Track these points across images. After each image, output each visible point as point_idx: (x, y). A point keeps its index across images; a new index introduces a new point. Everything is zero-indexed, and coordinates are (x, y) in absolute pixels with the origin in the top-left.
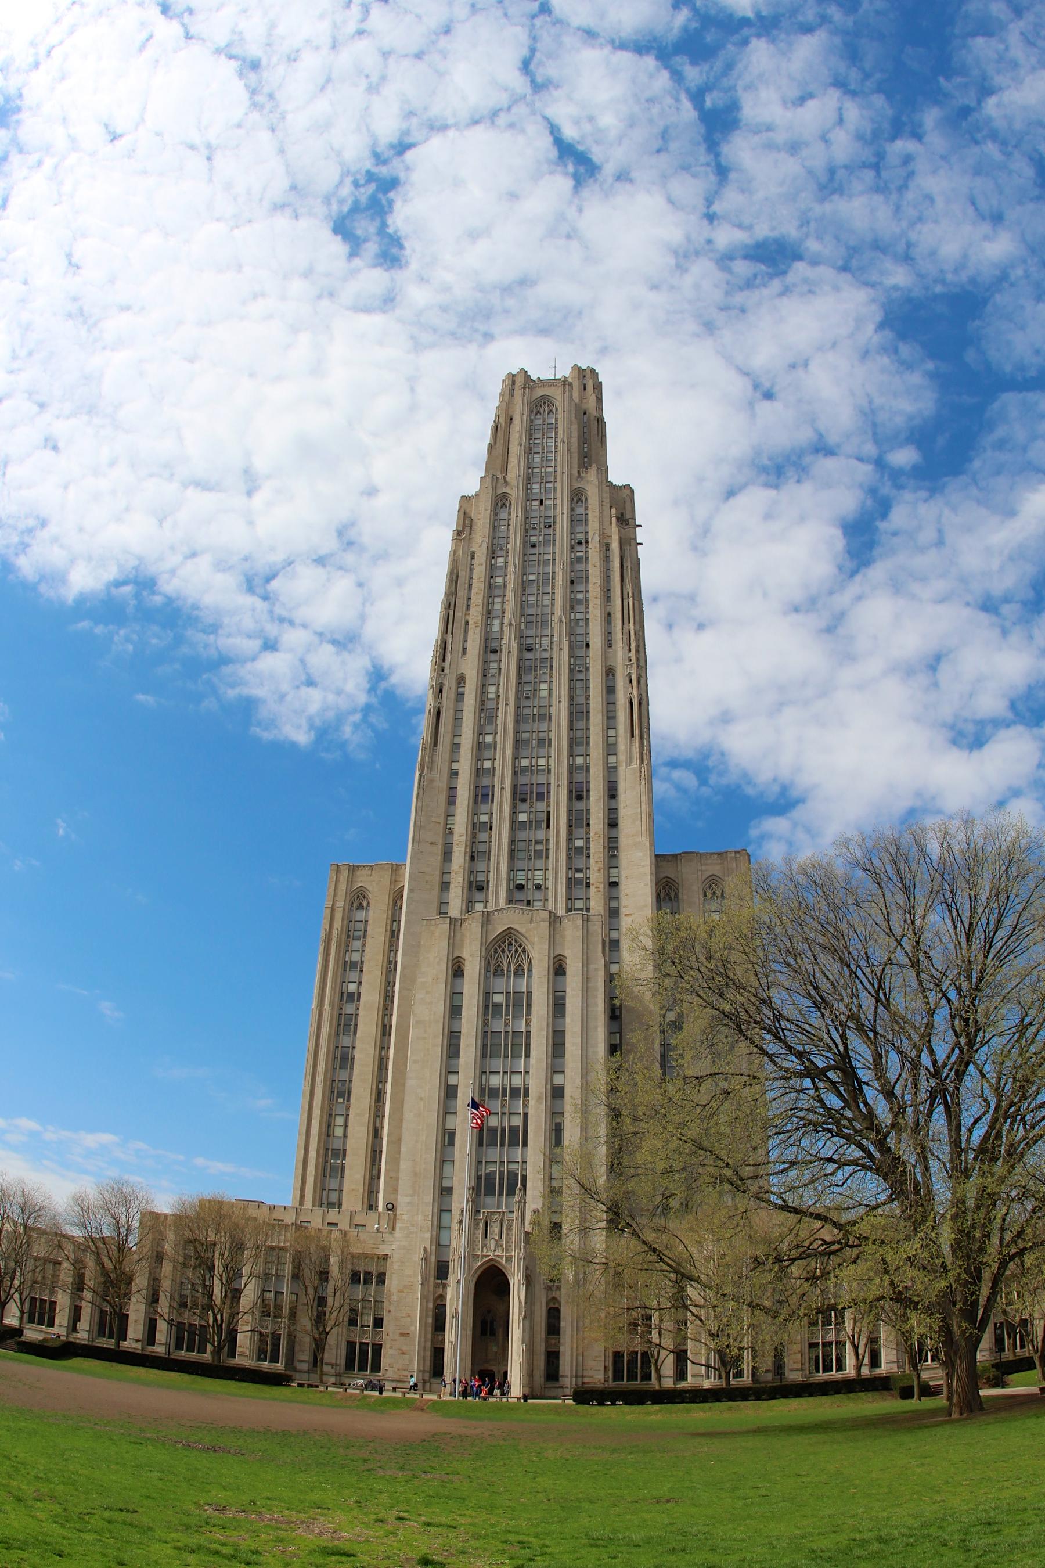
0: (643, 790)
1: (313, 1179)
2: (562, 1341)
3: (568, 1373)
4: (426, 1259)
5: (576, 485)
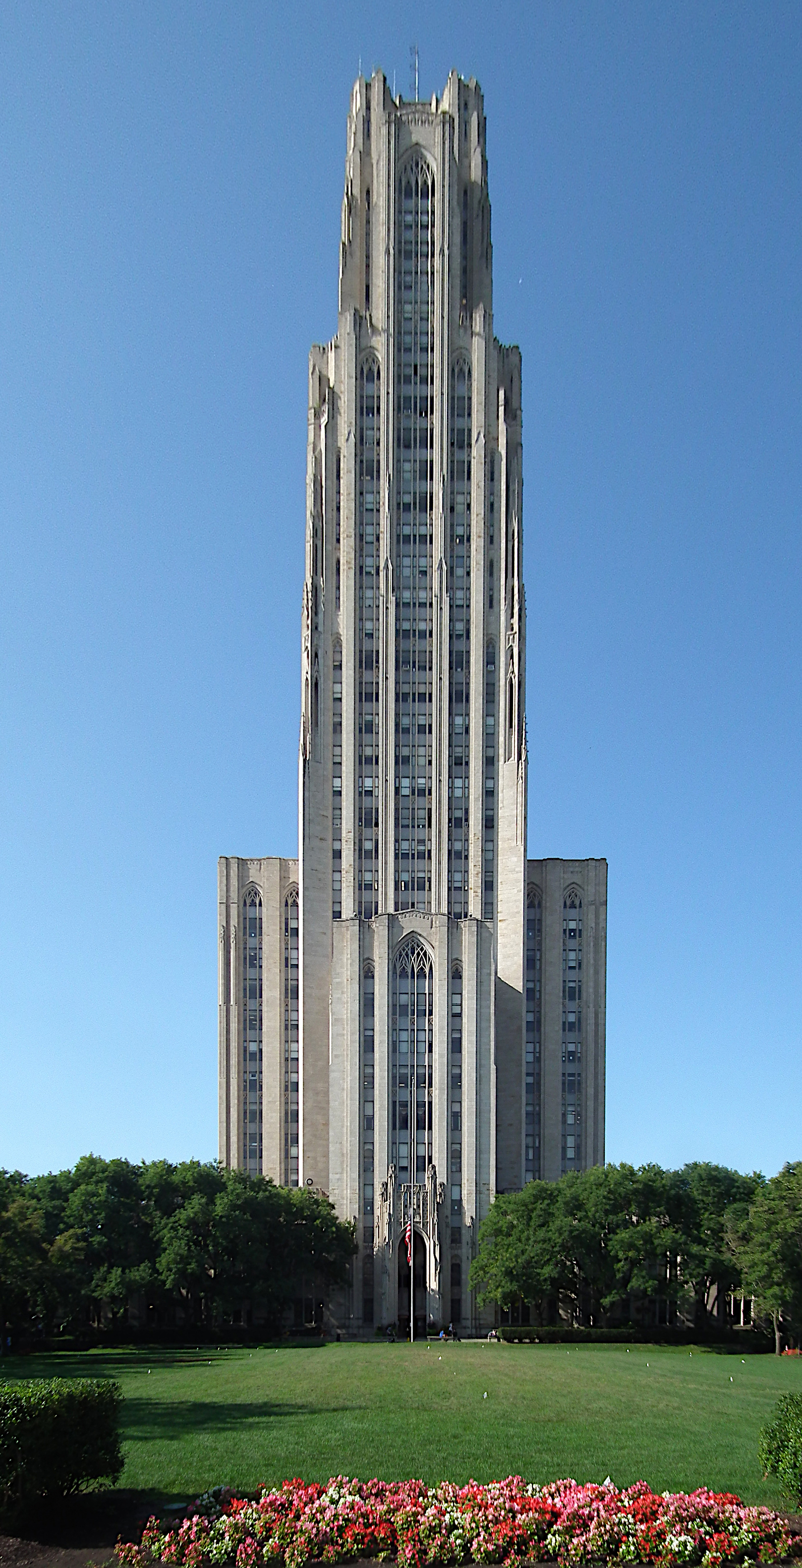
0: (520, 789)
2: (463, 1290)
3: (469, 1316)
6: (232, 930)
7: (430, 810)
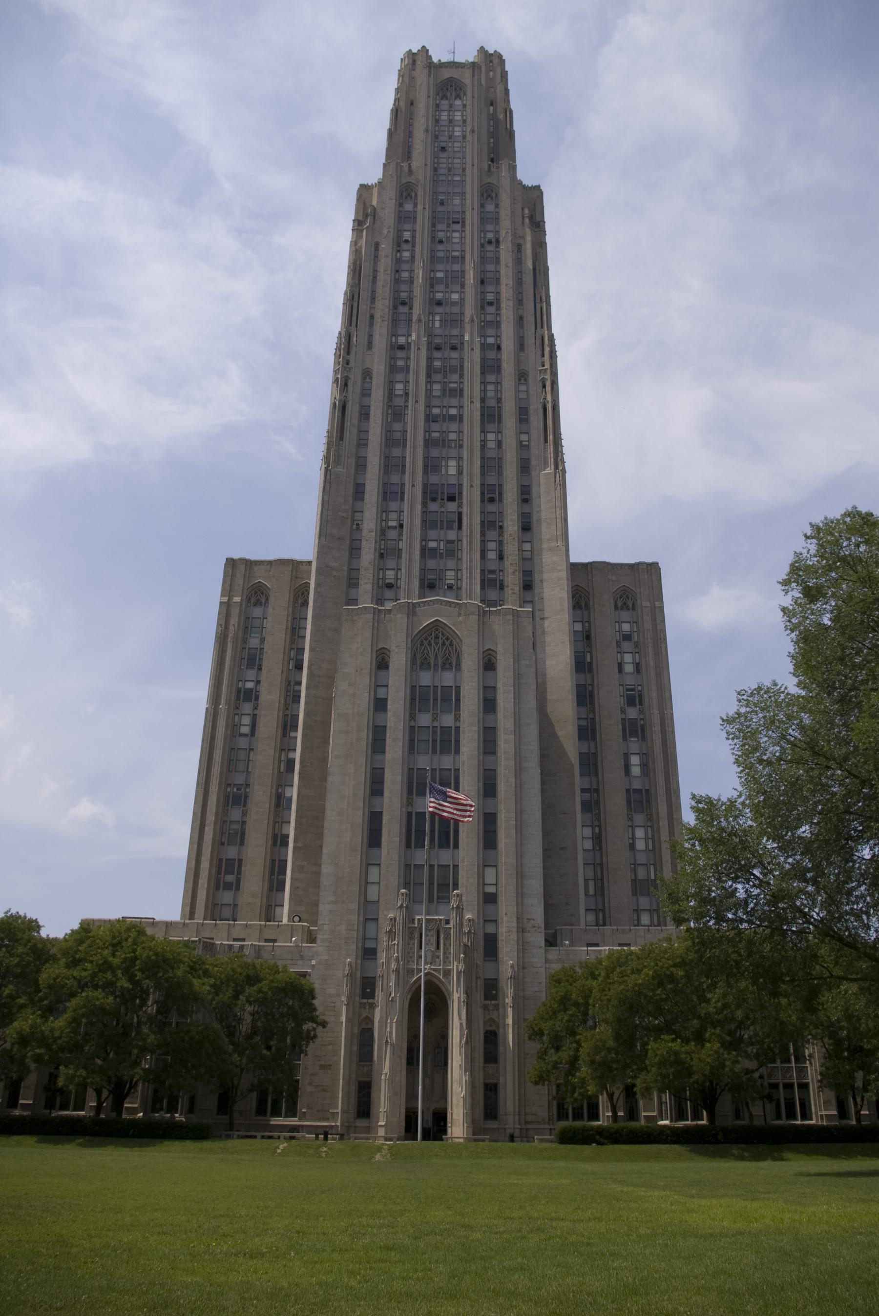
1: (205, 892)
4: (351, 976)
5: (487, 180)
6: (231, 628)
7: (460, 514)
